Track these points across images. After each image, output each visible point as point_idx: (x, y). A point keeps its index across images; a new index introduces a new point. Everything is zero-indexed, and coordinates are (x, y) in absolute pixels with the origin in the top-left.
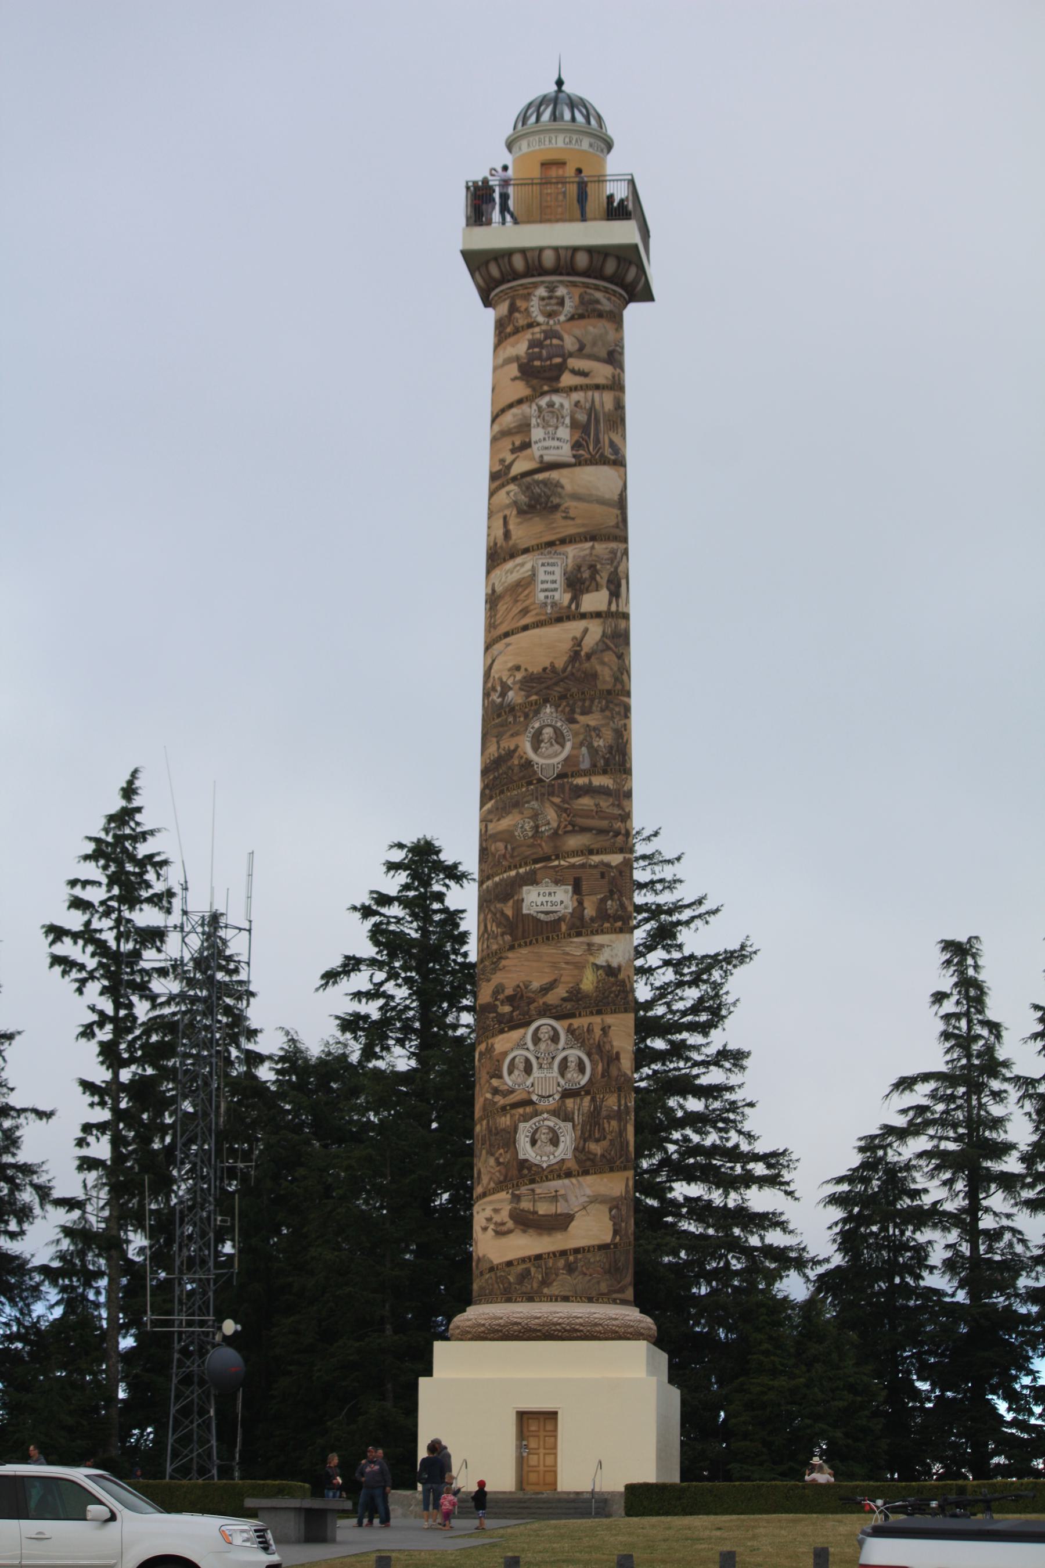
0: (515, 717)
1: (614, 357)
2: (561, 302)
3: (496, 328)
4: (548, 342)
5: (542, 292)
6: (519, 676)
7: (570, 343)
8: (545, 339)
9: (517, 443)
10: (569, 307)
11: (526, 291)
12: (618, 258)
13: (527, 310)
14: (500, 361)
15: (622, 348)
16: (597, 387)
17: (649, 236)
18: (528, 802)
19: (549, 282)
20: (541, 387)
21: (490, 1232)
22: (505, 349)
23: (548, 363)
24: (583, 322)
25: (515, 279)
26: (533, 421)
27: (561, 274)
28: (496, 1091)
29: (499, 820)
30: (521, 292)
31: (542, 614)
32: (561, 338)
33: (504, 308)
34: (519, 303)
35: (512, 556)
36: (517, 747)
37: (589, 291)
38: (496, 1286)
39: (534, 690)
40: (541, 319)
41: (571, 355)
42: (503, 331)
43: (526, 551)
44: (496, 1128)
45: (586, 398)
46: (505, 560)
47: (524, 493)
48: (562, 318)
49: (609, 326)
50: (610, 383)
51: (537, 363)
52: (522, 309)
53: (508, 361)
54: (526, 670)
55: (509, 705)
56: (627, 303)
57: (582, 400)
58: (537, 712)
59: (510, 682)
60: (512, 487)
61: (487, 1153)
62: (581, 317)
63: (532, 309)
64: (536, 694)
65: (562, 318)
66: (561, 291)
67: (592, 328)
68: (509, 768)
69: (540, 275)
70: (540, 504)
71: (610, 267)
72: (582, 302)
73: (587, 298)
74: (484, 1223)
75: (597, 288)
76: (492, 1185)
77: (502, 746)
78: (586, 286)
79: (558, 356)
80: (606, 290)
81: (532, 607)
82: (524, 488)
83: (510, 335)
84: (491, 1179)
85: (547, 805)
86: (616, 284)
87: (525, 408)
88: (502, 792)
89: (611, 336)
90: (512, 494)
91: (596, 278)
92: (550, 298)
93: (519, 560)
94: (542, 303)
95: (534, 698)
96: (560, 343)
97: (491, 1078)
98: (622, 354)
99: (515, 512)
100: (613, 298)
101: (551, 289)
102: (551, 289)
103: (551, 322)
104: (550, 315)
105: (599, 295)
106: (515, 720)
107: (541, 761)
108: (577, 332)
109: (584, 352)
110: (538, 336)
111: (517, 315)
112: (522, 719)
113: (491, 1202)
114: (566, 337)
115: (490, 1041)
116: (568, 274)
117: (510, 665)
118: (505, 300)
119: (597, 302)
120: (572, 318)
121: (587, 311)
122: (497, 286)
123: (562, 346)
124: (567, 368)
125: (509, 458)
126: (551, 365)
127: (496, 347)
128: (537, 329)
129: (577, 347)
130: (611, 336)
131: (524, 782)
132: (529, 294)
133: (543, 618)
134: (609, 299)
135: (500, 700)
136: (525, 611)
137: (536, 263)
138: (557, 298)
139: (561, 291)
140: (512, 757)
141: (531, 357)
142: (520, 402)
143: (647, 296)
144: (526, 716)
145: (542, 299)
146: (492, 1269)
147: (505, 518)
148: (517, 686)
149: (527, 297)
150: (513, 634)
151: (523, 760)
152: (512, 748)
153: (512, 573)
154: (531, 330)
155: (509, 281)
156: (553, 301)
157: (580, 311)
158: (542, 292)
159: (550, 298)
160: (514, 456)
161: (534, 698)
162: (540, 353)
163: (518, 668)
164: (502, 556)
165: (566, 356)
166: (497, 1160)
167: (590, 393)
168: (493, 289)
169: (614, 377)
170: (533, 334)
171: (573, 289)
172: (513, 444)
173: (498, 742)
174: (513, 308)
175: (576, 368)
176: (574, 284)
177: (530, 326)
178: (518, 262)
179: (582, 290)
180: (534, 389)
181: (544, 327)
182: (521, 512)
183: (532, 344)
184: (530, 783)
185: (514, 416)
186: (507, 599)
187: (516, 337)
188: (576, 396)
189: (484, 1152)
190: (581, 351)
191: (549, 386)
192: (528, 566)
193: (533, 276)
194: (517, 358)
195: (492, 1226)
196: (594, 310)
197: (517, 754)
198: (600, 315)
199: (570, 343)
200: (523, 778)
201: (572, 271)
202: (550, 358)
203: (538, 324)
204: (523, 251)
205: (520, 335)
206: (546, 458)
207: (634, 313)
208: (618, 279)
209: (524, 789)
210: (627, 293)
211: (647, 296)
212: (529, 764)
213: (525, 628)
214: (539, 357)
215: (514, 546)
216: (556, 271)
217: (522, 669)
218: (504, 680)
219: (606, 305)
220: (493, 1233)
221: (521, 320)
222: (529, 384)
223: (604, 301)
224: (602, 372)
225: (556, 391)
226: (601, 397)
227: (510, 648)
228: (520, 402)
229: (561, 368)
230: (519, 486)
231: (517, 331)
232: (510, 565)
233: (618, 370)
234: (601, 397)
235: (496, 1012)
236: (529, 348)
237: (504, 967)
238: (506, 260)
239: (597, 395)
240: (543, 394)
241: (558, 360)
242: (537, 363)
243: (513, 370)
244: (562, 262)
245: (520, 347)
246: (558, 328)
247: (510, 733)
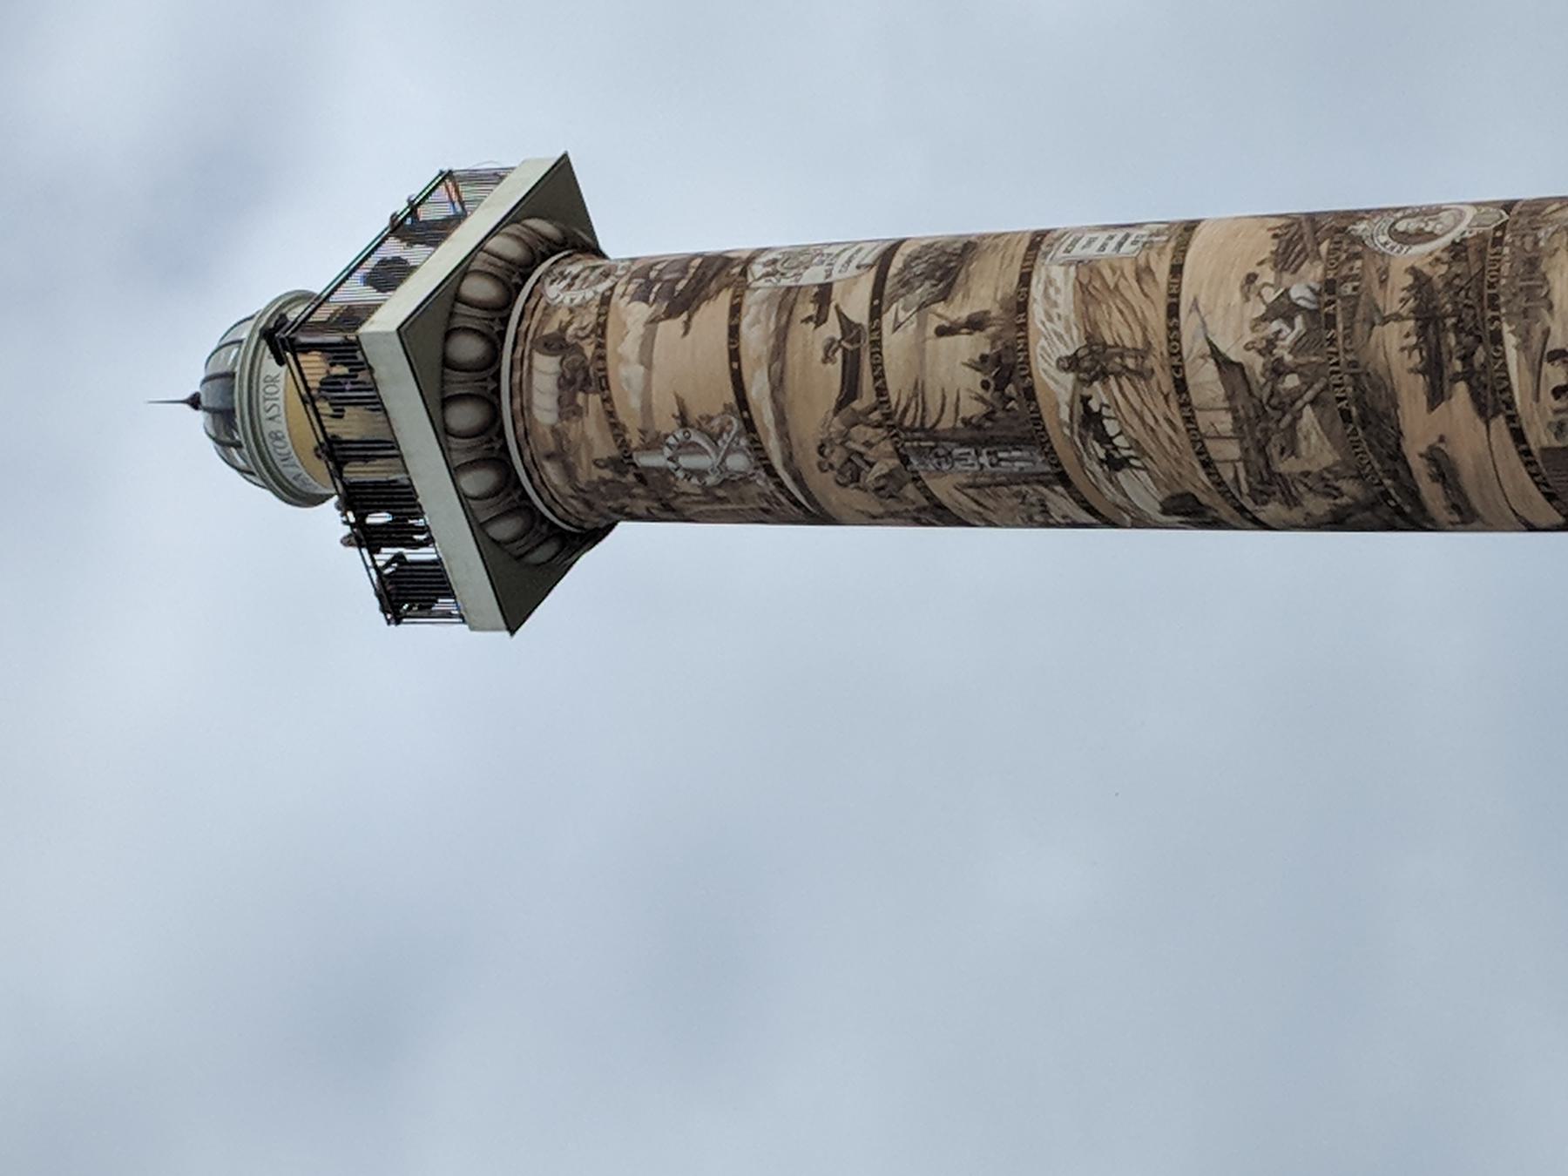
0: (1346, 279)
5: (553, 291)
6: (1267, 275)
9: (811, 310)
18: (1536, 243)
20: (728, 275)
22: (621, 359)
23: (692, 271)
26: (785, 282)
29: (1550, 307)
31: (1164, 248)
35: (1023, 307)
36: (1413, 271)
39: (1309, 246)
40: (603, 287)
43: (1025, 279)
46: (1023, 326)
47: (912, 290)
54: (1261, 263)
55: (1317, 294)
58: (1358, 240)
59: (1270, 295)
60: (887, 319)
63: (576, 302)
64: (1319, 244)
68: (1449, 284)
70: (949, 261)
77: (1393, 306)
81: (1142, 262)
82: (903, 291)
85: (1556, 215)
87: (751, 301)
88: (1494, 297)
90: (902, 316)
93: (1036, 289)
95: (1324, 248)
99: (940, 308)
104: (606, 275)
106: (1355, 278)
107: (1462, 227)
110: (632, 287)
112: (1358, 263)
117: (1237, 297)
125: (832, 329)
128: (619, 290)
131: (1490, 251)
133: (1172, 244)
135: (1299, 320)
136: (1143, 273)
137: (500, 263)
140: (1430, 279)
142: (735, 310)
144: (1357, 256)
147: (941, 332)
148: (1286, 277)
150: (1177, 296)
151: (1446, 256)
152: (1409, 280)
153: (1055, 305)
154: (614, 299)
160: (832, 314)
161: (1324, 248)
163: (1251, 278)
164: (1011, 334)
172: (810, 319)
173: (1385, 321)
177: (606, 300)
180: (728, 286)
182: (944, 296)
184: (1498, 242)
185: (756, 321)
186: (1100, 314)
192: (1057, 272)
197: (1427, 270)
200: (1481, 252)
203: (612, 289)
206: (869, 260)
209: (1506, 250)
212: (1457, 250)
213: (1177, 270)
214: (677, 281)
215: (1004, 306)
217: (1257, 270)
218: (1263, 309)
222: (708, 298)
227: (1202, 302)
228: (735, 310)
230: (893, 300)
232: (1037, 310)
236: (646, 300)
242: (680, 286)
247: (1376, 285)
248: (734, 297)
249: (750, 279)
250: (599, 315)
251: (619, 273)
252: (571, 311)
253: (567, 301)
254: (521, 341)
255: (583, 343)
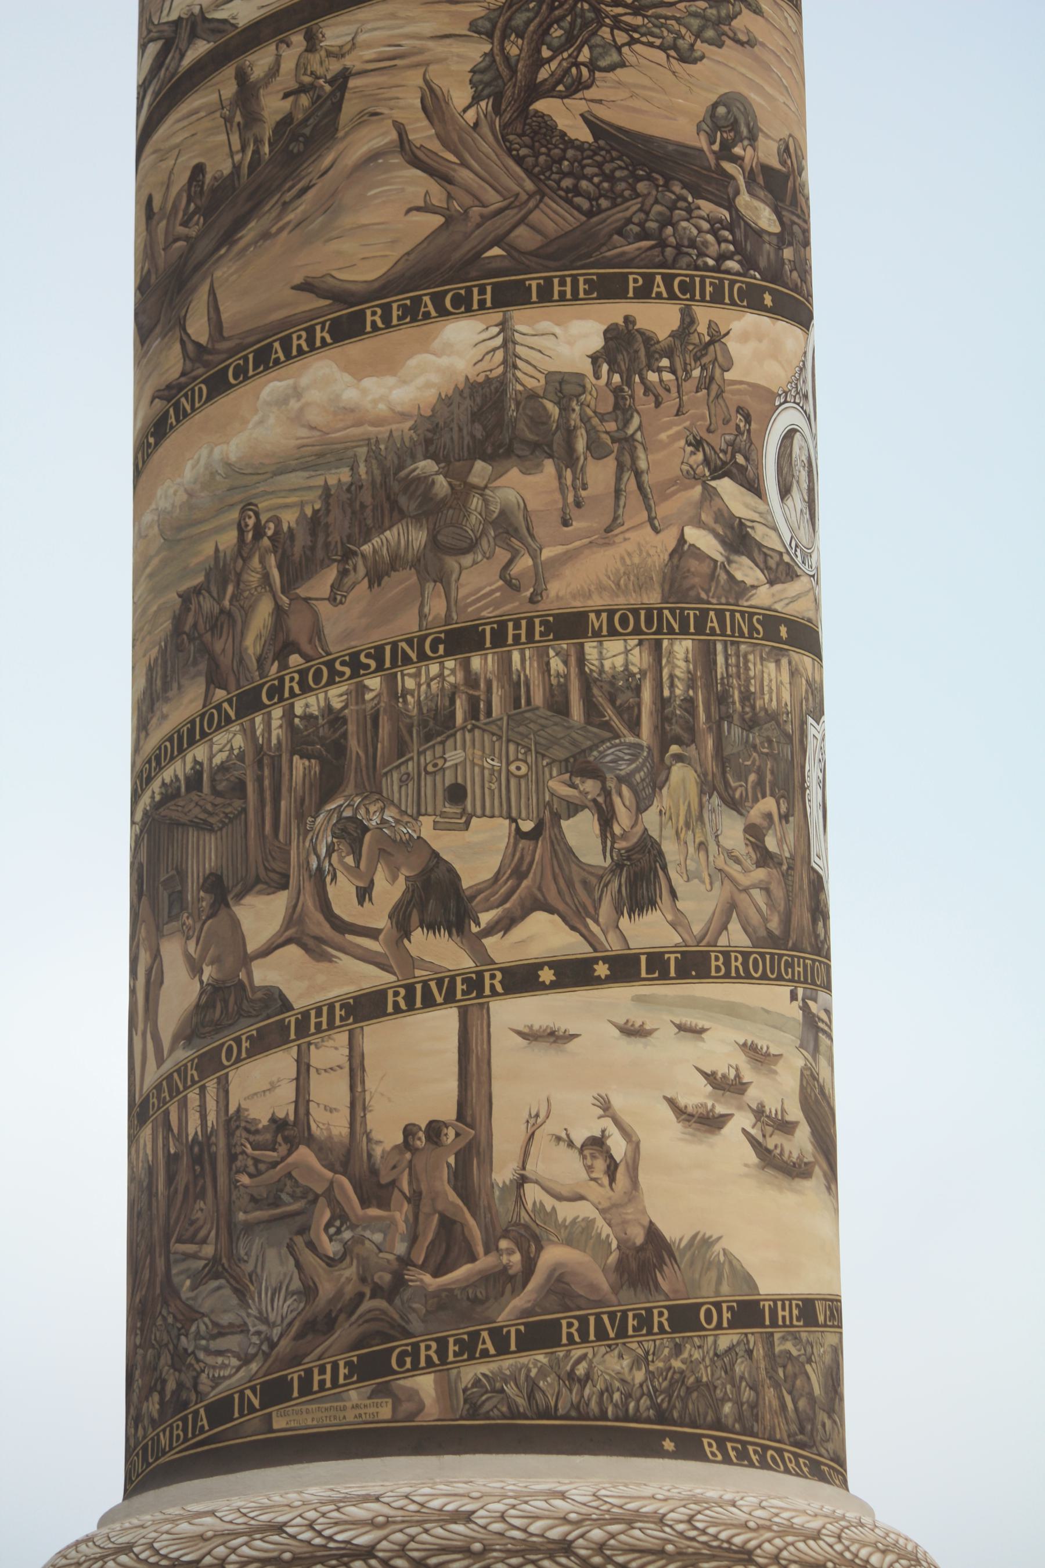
21: (733, 1144)
28: (738, 538)
38: (770, 1394)
44: (747, 697)
61: (706, 787)
74: (697, 1094)
76: (736, 937)
84: (732, 907)
97: (719, 471)
113: (732, 1011)
115: (704, 314)
146: (749, 1313)
166: (755, 834)
189: (682, 777)
195: (742, 1120)
220: (752, 1158)
235: (731, 206)
237: (750, 43)
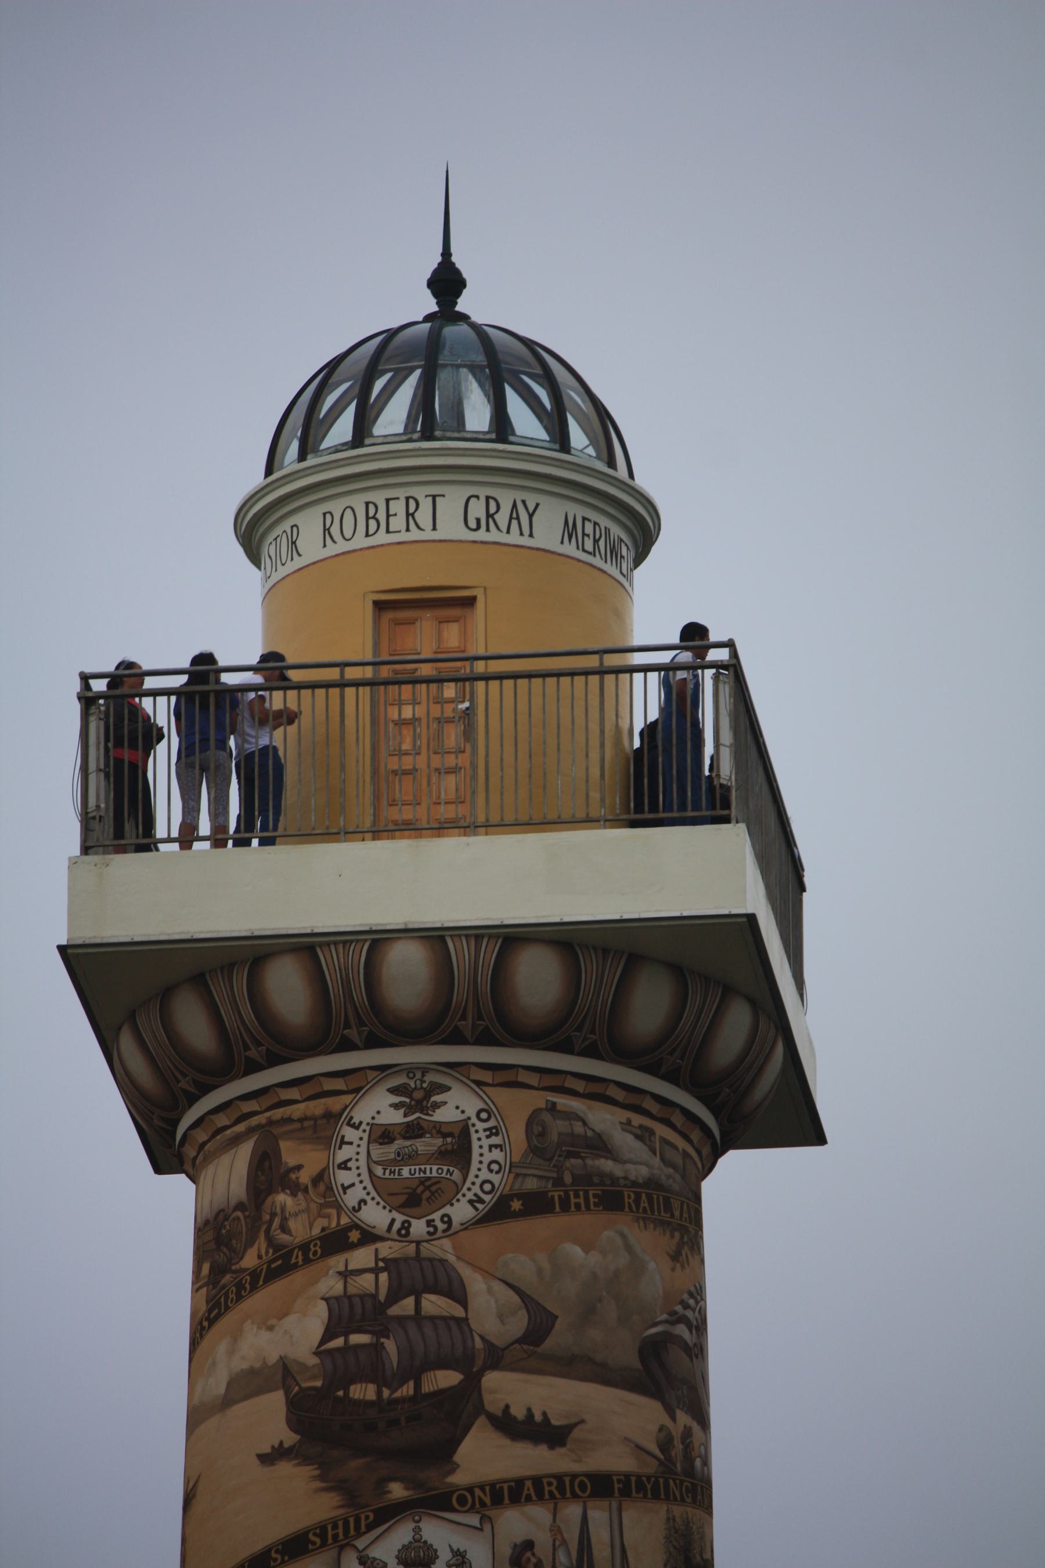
1: (669, 1363)
2: (457, 1147)
3: (201, 1254)
4: (406, 1306)
7: (490, 1311)
8: (395, 1295)
10: (488, 1164)
11: (316, 1108)
12: (679, 972)
13: (321, 1178)
14: (217, 1384)
15: (700, 1327)
16: (601, 1486)
17: (803, 888)
19: (410, 1070)
20: (382, 1483)
22: (236, 1336)
23: (408, 1390)
24: (542, 1226)
25: (274, 1060)
27: (456, 1038)
30: (297, 1111)
32: (458, 1293)
33: (232, 1171)
34: (293, 1153)
37: (563, 1101)
41: (496, 1358)
42: (229, 1266)
45: (556, 1530)
48: (461, 1211)
49: (650, 1243)
50: (651, 1468)
51: (363, 1392)
52: (304, 1177)
53: (247, 1385)
56: (718, 1152)
57: (543, 1540)
62: (536, 1205)
65: (461, 1211)
66: (457, 1104)
67: (580, 1250)
69: (373, 1042)
71: (649, 1007)
72: (539, 1142)
73: (558, 1127)
75: (597, 1091)
78: (555, 1082)
79: (443, 1364)
80: (633, 1100)
83: (257, 1280)
86: (672, 1078)
89: (657, 1278)
91: (591, 1052)
92: (413, 1131)
94: (377, 1152)
96: (458, 1311)
98: (698, 1352)
100: (662, 1131)
101: (419, 1097)
102: (419, 1097)
103: (419, 1228)
104: (413, 1199)
105: (603, 1119)
108: (522, 1266)
109: (548, 1345)
110: (366, 1282)
111: (283, 1199)
114: (476, 1284)
116: (485, 1039)
118: (236, 1141)
119: (600, 1145)
120: (498, 1212)
121: (559, 1182)
122: (206, 1089)
123: (462, 1322)
124: (480, 1409)
126: (418, 1396)
127: (201, 1329)
128: (362, 1257)
129: (519, 1324)
130: (657, 1278)
132: (332, 1117)
134: (644, 1135)
137: (360, 995)
138: (440, 1130)
139: (457, 1104)
141: (341, 1368)
143: (796, 1122)
145: (383, 1135)
149: (324, 1129)
154: (337, 1262)
155: (252, 1068)
156: (426, 1145)
157: (531, 1184)
158: (380, 1107)
159: (413, 1131)
162: (377, 1348)
165: (476, 1361)
167: (572, 1511)
168: (192, 1100)
169: (666, 1444)
170: (346, 1274)
171: (503, 1096)
174: (268, 1175)
175: (518, 1412)
176: (507, 1077)
177: (336, 1242)
178: (288, 991)
179: (538, 1099)
181: (386, 1249)
183: (344, 1315)
187: (278, 1287)
188: (517, 1523)
190: (532, 1344)
191: (410, 1483)
193: (346, 1046)
194: (285, 1372)
196: (585, 1179)
198: (611, 1198)
199: (490, 1311)
201: (501, 1024)
202: (414, 1372)
203: (369, 1237)
204: (307, 948)
205: (297, 1278)
207: (743, 1190)
208: (673, 1054)
210: (716, 1112)
211: (796, 1122)
214: (375, 1374)
216: (434, 1026)
219: (635, 1159)
221: (299, 1220)
223: (625, 1142)
224: (620, 1424)
225: (439, 1502)
226: (618, 1528)
229: (460, 1410)
231: (283, 1263)
233: (683, 1418)
234: (618, 1528)
238: (240, 981)
239: (599, 1516)
240: (388, 1514)
241: (447, 1379)
243: (269, 1418)
244: (460, 993)
245: (295, 1327)
246: (444, 1248)
248: (321, 1530)
249: (361, 1543)
250: (305, 1247)
251: (419, 1228)
252: (321, 1178)
253: (342, 1155)
254: (268, 1100)
255: (262, 1243)
